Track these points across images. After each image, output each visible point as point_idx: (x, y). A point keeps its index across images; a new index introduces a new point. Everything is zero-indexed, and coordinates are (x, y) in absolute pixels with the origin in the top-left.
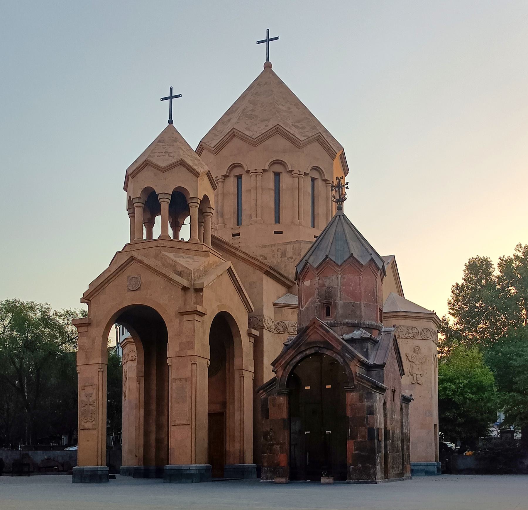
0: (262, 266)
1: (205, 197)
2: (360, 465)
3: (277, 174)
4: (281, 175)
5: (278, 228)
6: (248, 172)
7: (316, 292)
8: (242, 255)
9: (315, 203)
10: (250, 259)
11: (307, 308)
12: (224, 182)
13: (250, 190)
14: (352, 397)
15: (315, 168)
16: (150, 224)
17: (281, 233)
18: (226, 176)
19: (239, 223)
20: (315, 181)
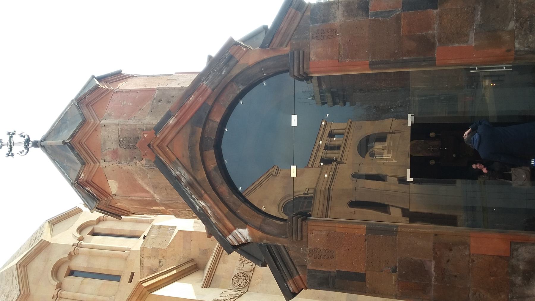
2: (512, 25)
5: (125, 278)
7: (126, 167)
9: (118, 233)
11: (155, 187)
15: (80, 229)
17: (133, 274)
20: (97, 231)
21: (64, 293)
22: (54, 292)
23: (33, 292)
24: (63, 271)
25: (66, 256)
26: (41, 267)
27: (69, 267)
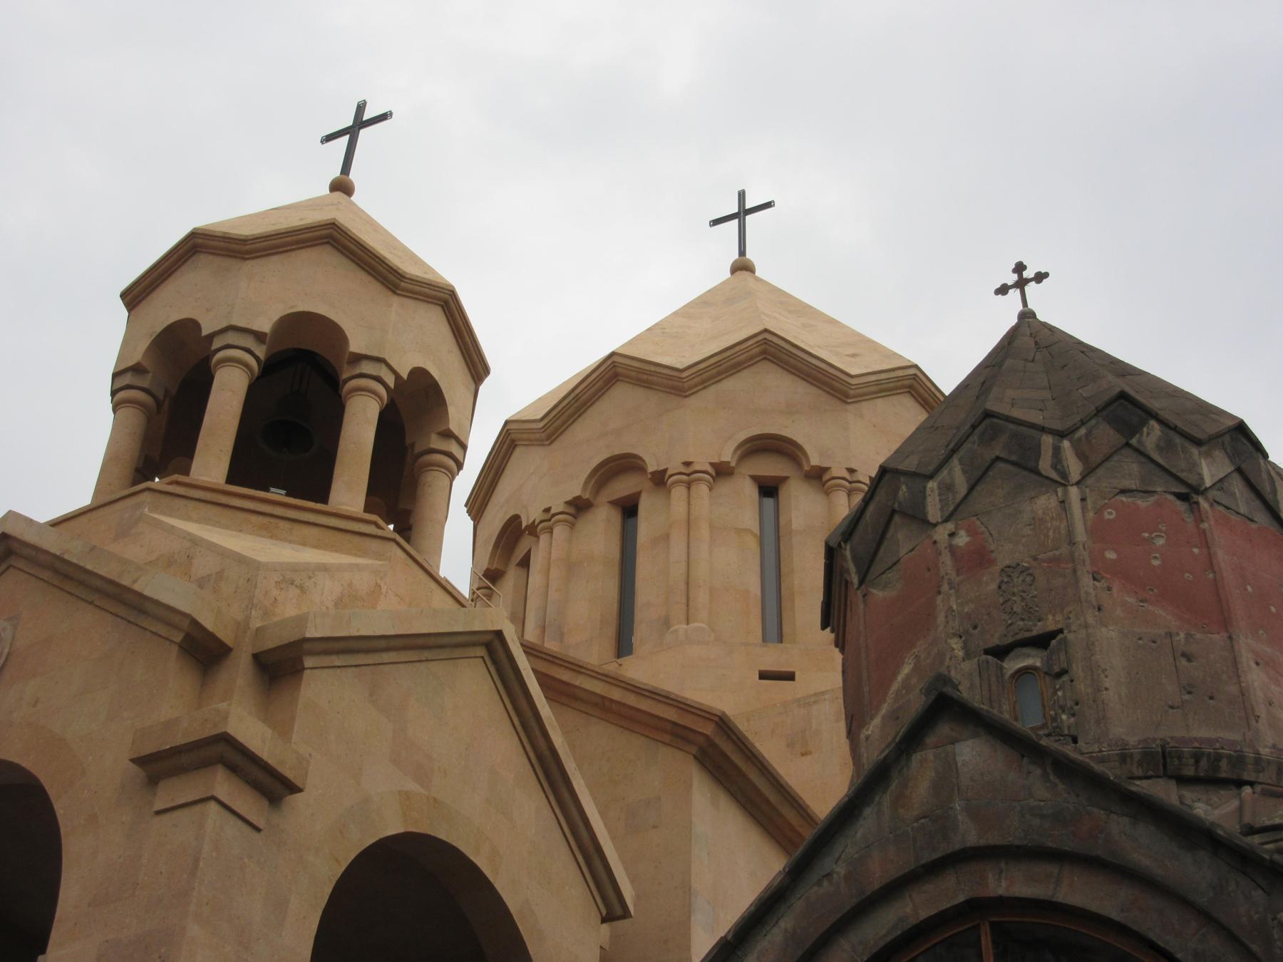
0: (687, 721)
3: (769, 489)
4: (783, 492)
5: (773, 659)
6: (660, 479)
8: (597, 687)
10: (631, 700)
12: (572, 526)
13: (666, 537)
17: (790, 677)
18: (579, 507)
21: (703, 488)
22: (702, 463)
23: (693, 401)
25: (815, 460)
26: (770, 402)
27: (784, 479)
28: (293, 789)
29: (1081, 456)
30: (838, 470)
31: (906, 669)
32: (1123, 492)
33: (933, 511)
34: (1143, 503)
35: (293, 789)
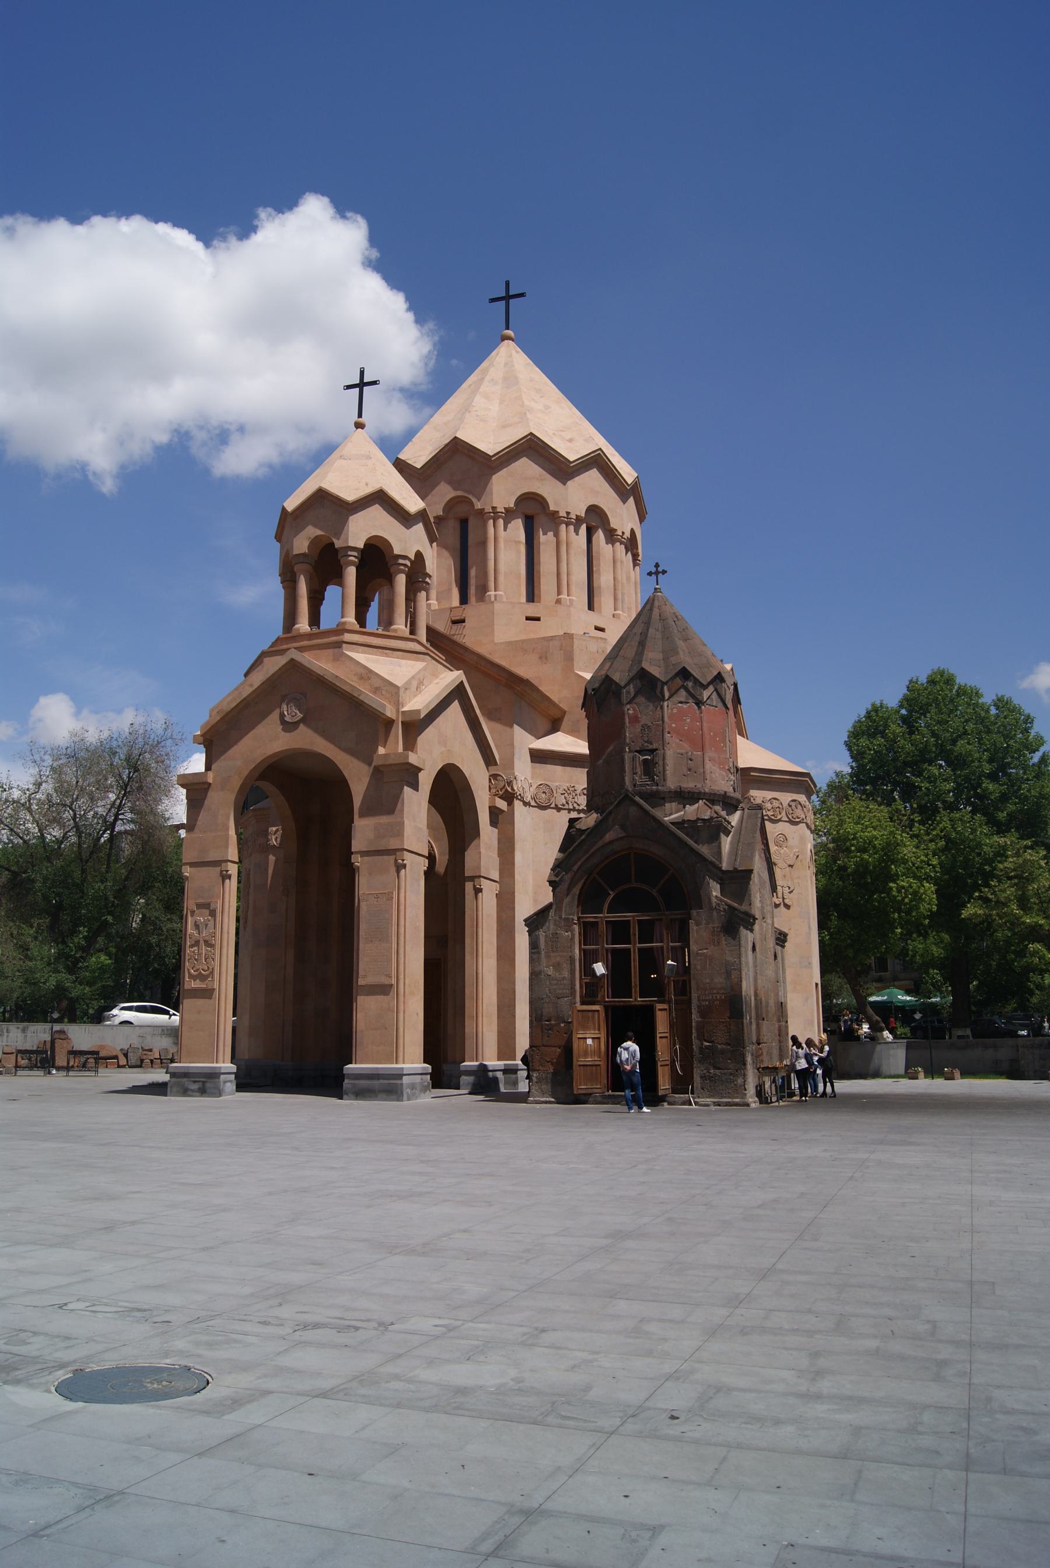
1: (419, 555)
5: (532, 610)
14: (699, 932)
16: (316, 600)
17: (538, 619)
19: (464, 600)
21: (501, 522)
24: (531, 509)
28: (420, 770)
29: (669, 690)
30: (563, 514)
31: (611, 748)
32: (681, 702)
33: (625, 700)
34: (685, 706)
35: (420, 770)
